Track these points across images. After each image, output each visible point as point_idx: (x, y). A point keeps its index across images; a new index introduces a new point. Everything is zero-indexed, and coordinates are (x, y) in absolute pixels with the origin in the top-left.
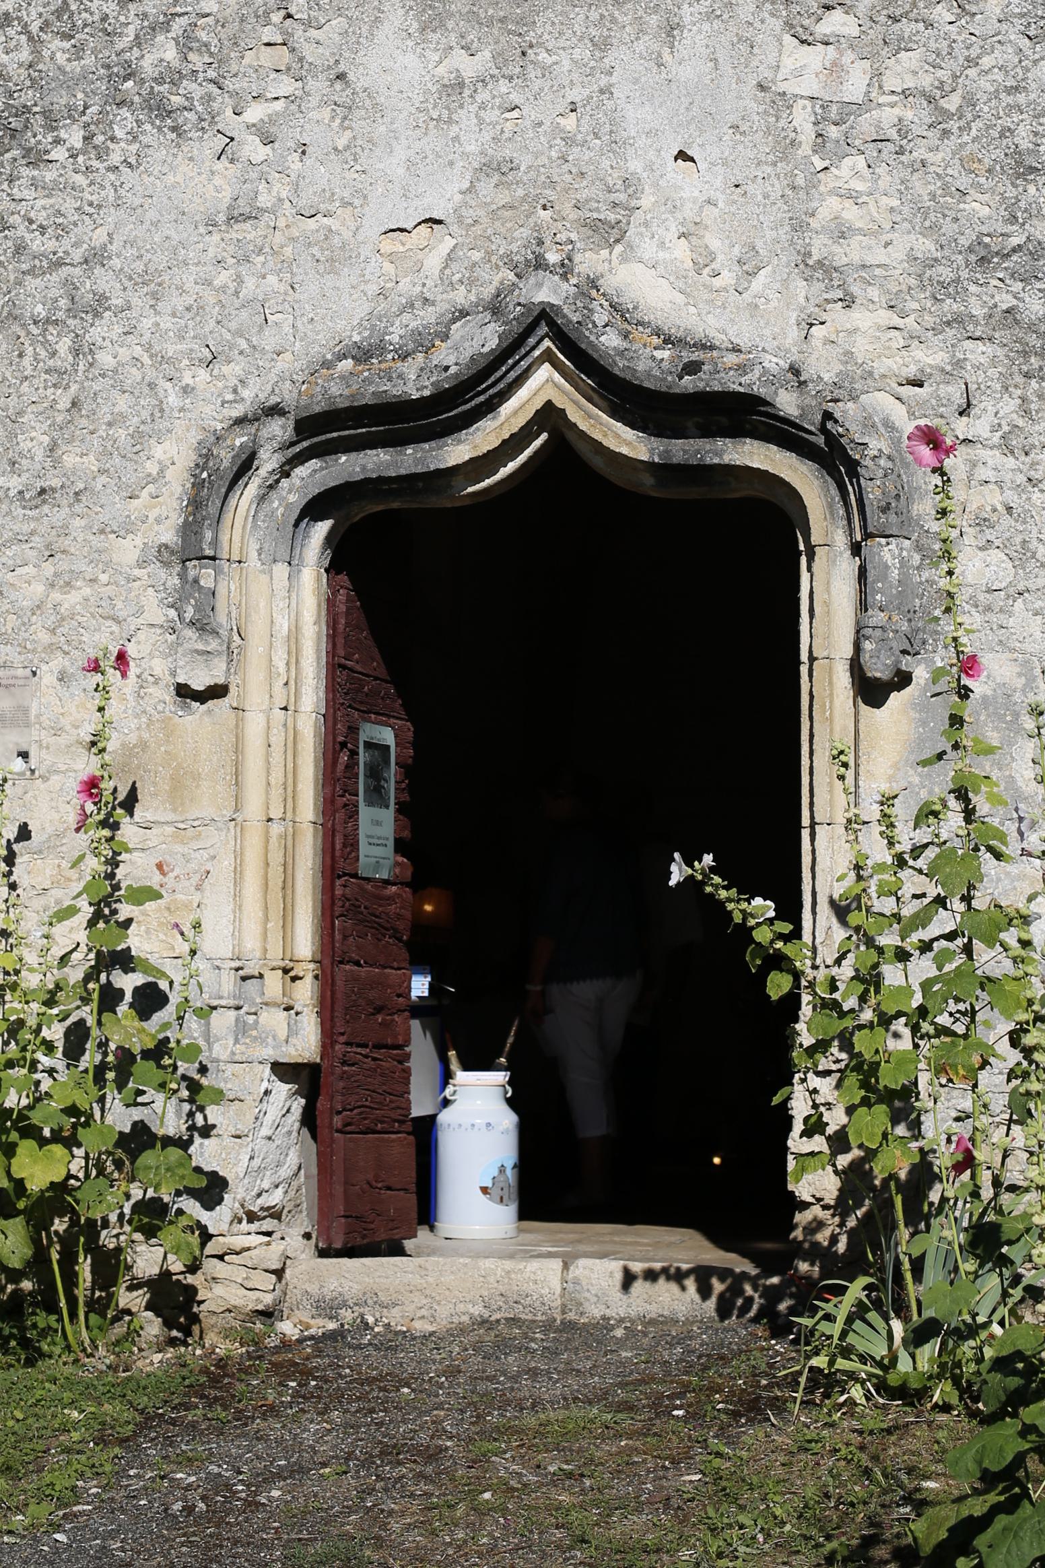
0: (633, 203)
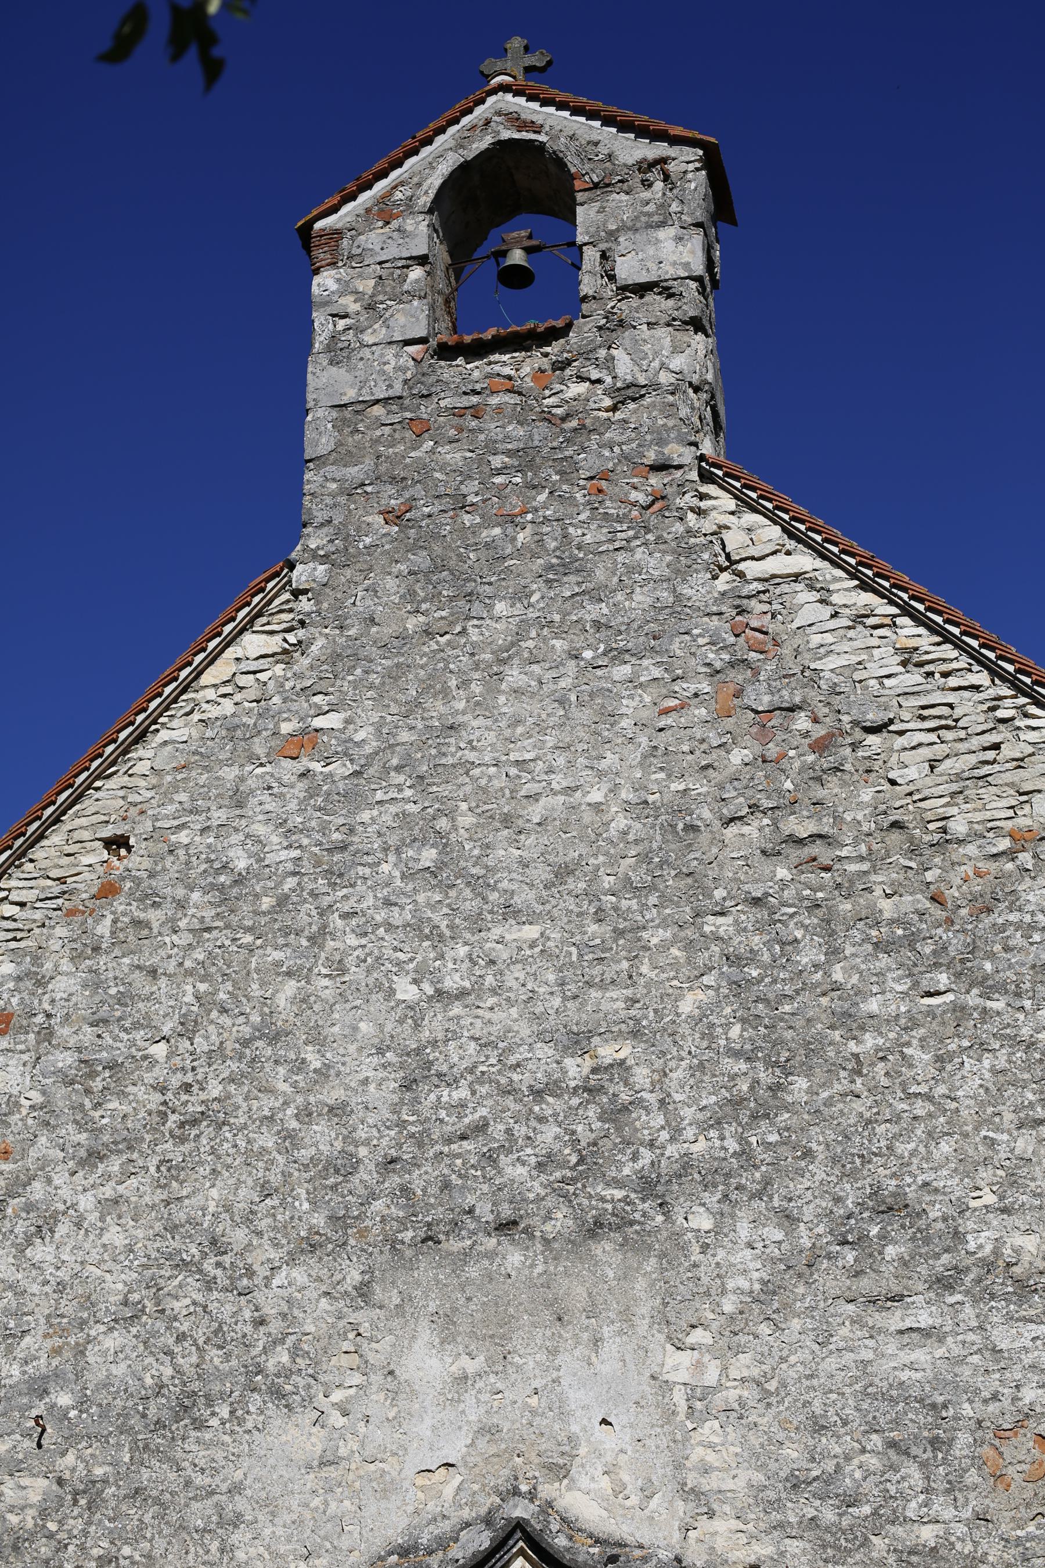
0: (574, 1452)
